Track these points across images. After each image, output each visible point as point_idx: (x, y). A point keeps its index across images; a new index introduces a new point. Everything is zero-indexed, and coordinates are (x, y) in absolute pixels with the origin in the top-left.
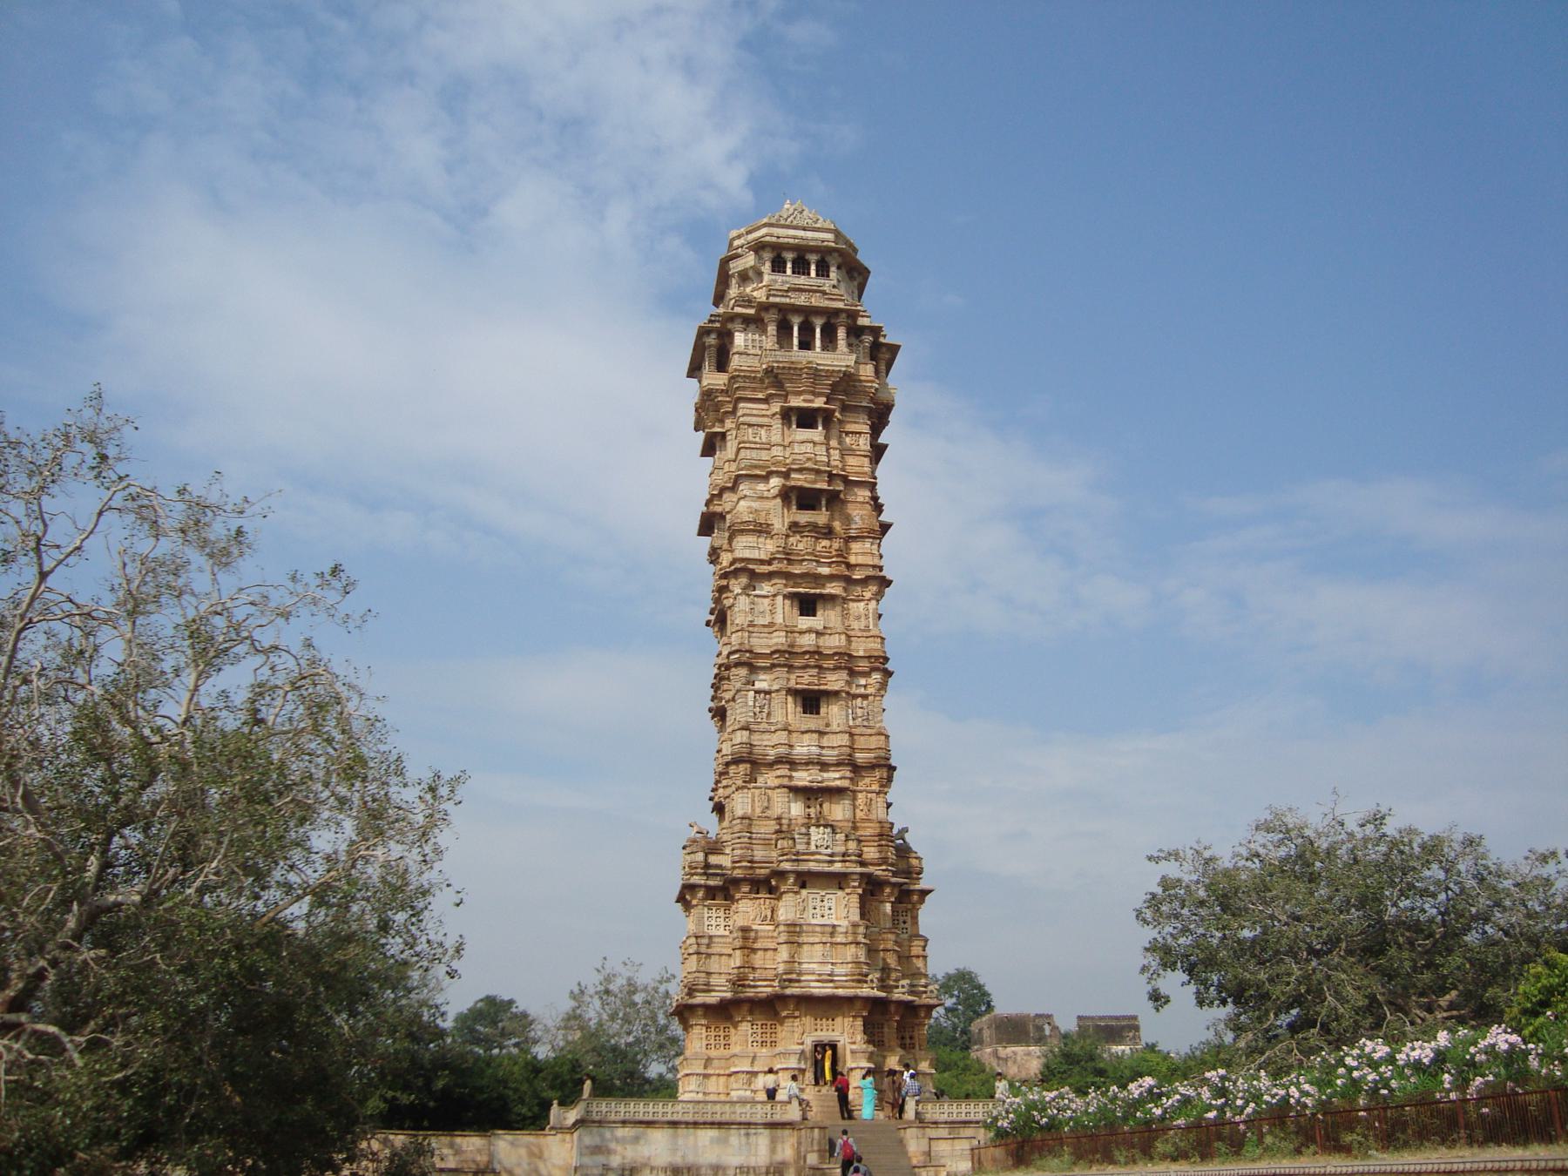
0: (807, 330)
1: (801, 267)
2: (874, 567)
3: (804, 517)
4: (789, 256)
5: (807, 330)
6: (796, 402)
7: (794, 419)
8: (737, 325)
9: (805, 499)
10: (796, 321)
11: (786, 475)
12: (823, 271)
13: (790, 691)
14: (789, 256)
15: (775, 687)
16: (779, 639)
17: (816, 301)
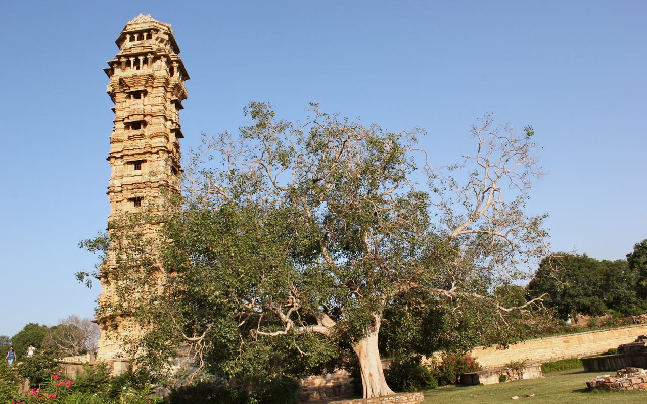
0: (137, 62)
1: (141, 38)
2: (162, 147)
3: (133, 132)
4: (136, 36)
5: (137, 62)
6: (132, 90)
7: (132, 96)
8: (115, 66)
9: (136, 125)
10: (132, 59)
11: (128, 118)
12: (149, 37)
13: (130, 200)
14: (136, 36)
15: (123, 198)
16: (126, 180)
17: (140, 50)
